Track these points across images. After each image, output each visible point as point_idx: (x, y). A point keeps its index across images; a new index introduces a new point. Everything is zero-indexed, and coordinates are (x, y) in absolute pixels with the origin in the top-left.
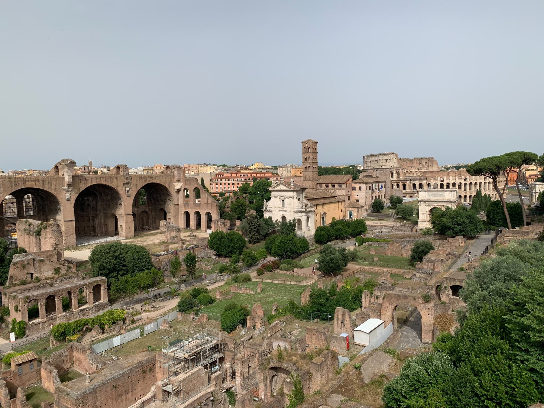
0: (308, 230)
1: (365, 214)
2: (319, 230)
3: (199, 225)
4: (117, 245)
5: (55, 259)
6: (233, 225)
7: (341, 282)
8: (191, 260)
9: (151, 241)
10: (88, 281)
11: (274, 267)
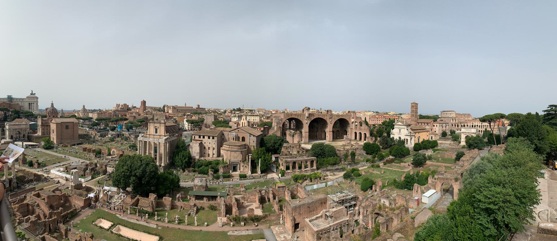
0: (410, 145)
1: (438, 137)
2: (416, 144)
3: (361, 139)
4: (322, 144)
5: (298, 147)
6: (376, 140)
7: (422, 171)
8: (353, 155)
9: (339, 144)
10: (309, 158)
11: (391, 161)
